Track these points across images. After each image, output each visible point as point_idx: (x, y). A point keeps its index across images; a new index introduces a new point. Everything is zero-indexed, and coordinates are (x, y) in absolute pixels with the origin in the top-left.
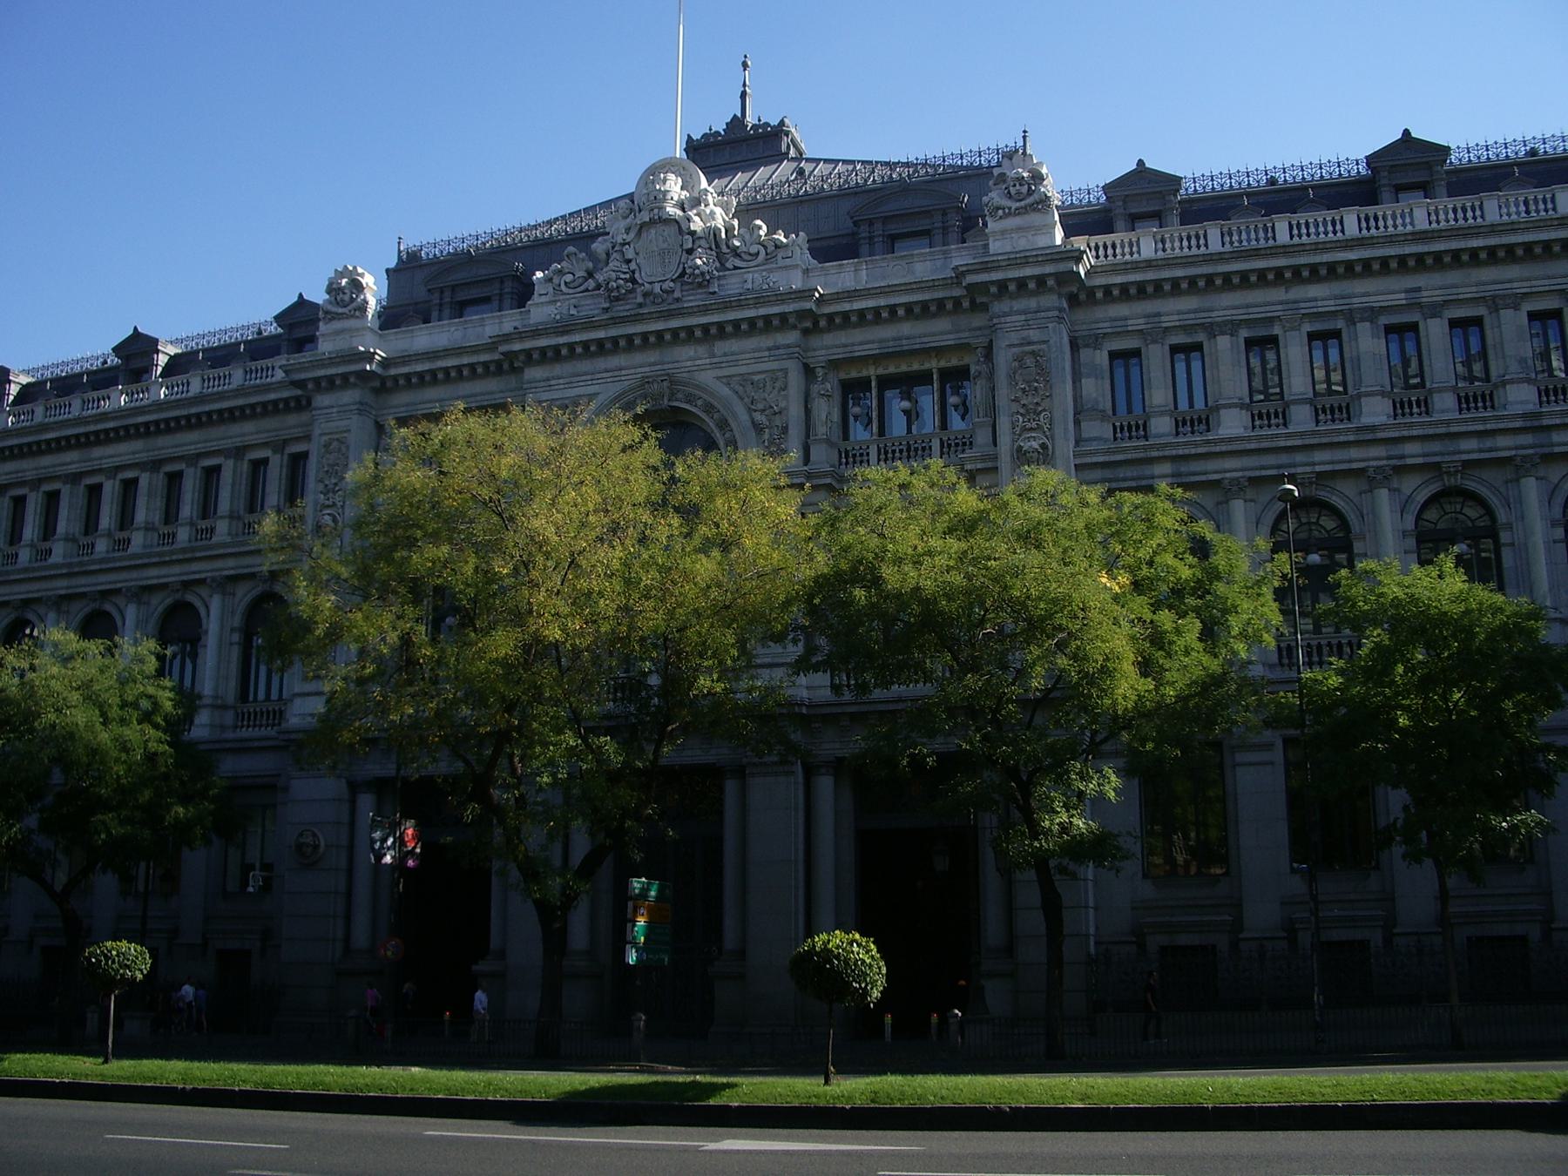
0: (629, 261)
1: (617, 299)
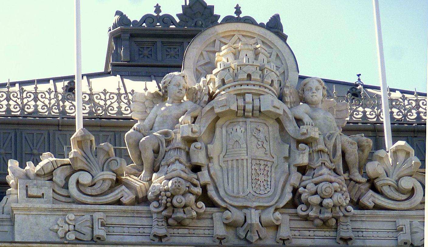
0: (196, 169)
1: (180, 224)
